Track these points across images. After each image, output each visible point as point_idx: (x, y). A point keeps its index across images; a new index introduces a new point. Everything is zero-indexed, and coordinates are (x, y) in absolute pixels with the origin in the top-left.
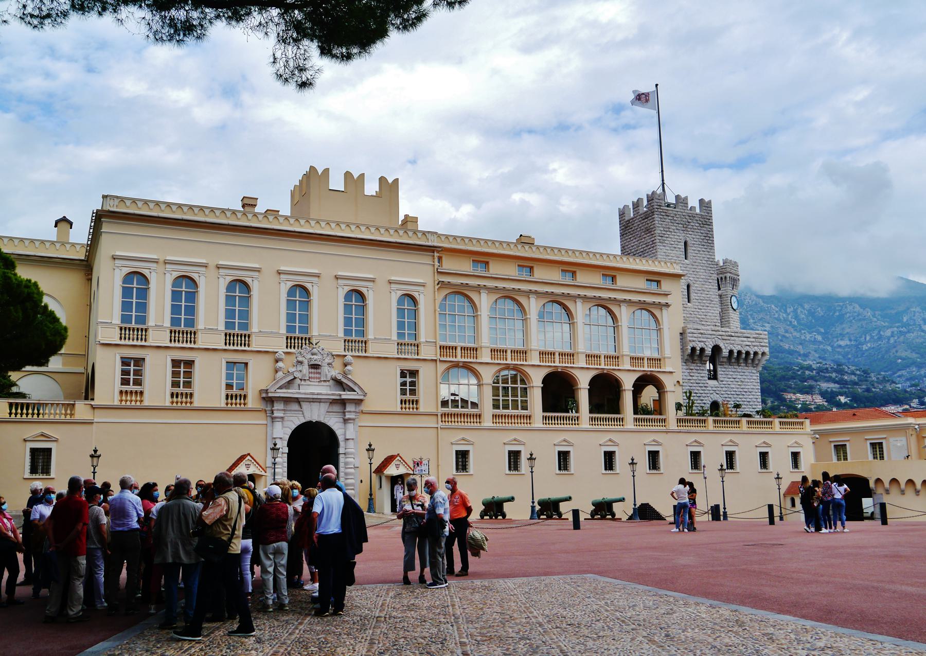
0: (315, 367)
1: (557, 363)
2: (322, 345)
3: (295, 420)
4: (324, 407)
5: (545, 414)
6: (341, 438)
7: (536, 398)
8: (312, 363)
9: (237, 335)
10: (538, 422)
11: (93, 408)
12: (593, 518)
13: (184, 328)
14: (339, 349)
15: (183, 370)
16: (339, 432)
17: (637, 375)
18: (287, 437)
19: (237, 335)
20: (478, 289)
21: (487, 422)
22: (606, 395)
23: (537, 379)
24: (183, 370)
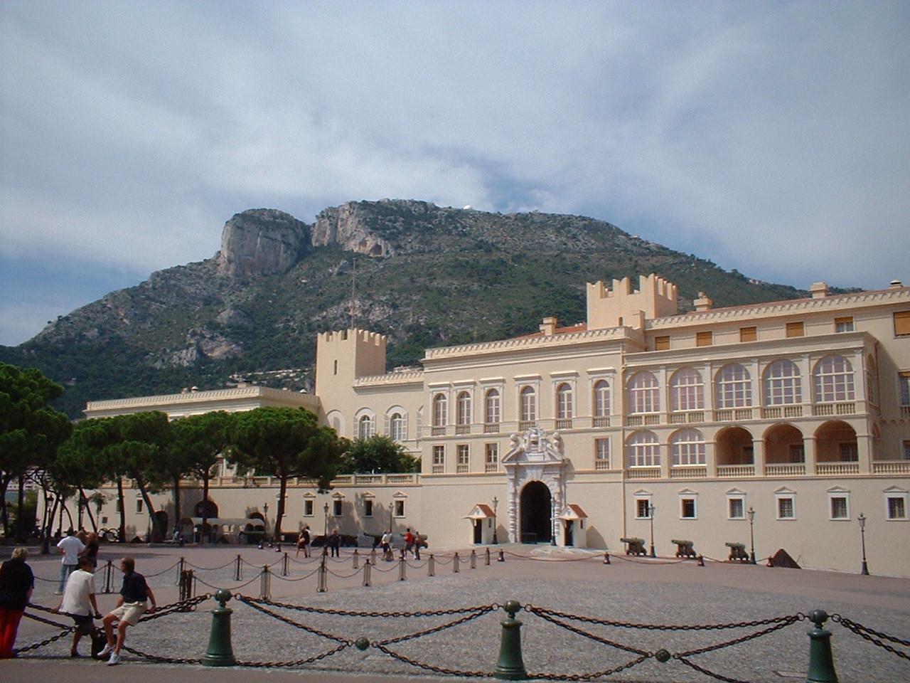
0: (535, 443)
1: (733, 421)
2: (540, 426)
3: (523, 482)
4: (540, 471)
5: (819, 464)
6: (552, 492)
7: (710, 452)
8: (532, 440)
9: (490, 424)
10: (711, 475)
11: (423, 477)
12: (730, 562)
13: (462, 426)
14: (551, 427)
15: (462, 449)
16: (550, 488)
17: (819, 424)
18: (519, 492)
19: (490, 424)
20: (657, 367)
21: (665, 477)
22: (785, 444)
23: (710, 436)
24: (462, 449)
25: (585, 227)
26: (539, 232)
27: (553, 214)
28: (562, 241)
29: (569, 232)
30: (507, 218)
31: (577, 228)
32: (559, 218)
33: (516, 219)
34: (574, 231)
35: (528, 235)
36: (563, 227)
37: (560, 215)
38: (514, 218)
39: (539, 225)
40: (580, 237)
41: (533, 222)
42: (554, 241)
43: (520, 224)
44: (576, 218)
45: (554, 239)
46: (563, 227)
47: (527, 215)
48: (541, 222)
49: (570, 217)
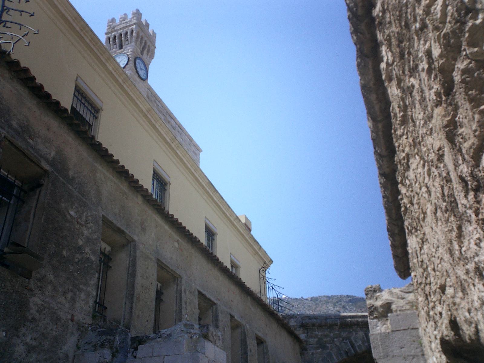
25: (350, 301)
26: (324, 306)
27: (332, 296)
28: (337, 310)
29: (341, 304)
30: (307, 300)
31: (345, 302)
32: (335, 297)
33: (311, 300)
34: (343, 304)
35: (318, 309)
36: (337, 302)
37: (336, 296)
38: (309, 299)
39: (324, 302)
40: (347, 307)
41: (321, 301)
42: (333, 311)
43: (313, 303)
44: (345, 296)
45: (332, 309)
46: (337, 302)
47: (317, 298)
48: (325, 301)
49: (341, 296)
